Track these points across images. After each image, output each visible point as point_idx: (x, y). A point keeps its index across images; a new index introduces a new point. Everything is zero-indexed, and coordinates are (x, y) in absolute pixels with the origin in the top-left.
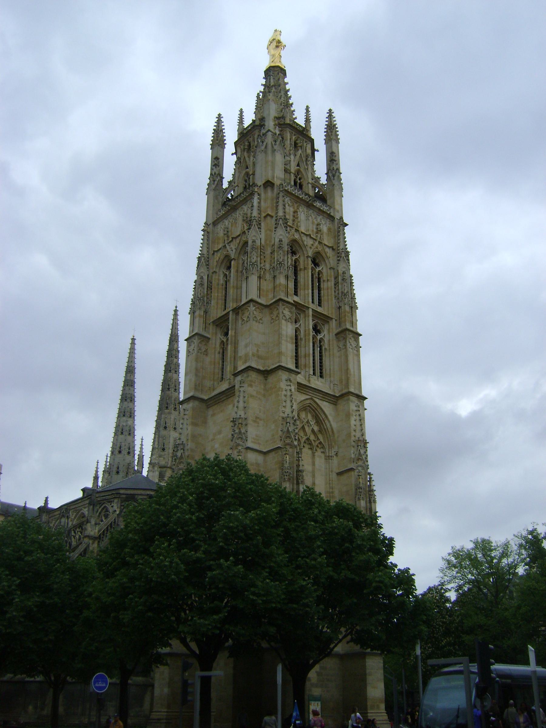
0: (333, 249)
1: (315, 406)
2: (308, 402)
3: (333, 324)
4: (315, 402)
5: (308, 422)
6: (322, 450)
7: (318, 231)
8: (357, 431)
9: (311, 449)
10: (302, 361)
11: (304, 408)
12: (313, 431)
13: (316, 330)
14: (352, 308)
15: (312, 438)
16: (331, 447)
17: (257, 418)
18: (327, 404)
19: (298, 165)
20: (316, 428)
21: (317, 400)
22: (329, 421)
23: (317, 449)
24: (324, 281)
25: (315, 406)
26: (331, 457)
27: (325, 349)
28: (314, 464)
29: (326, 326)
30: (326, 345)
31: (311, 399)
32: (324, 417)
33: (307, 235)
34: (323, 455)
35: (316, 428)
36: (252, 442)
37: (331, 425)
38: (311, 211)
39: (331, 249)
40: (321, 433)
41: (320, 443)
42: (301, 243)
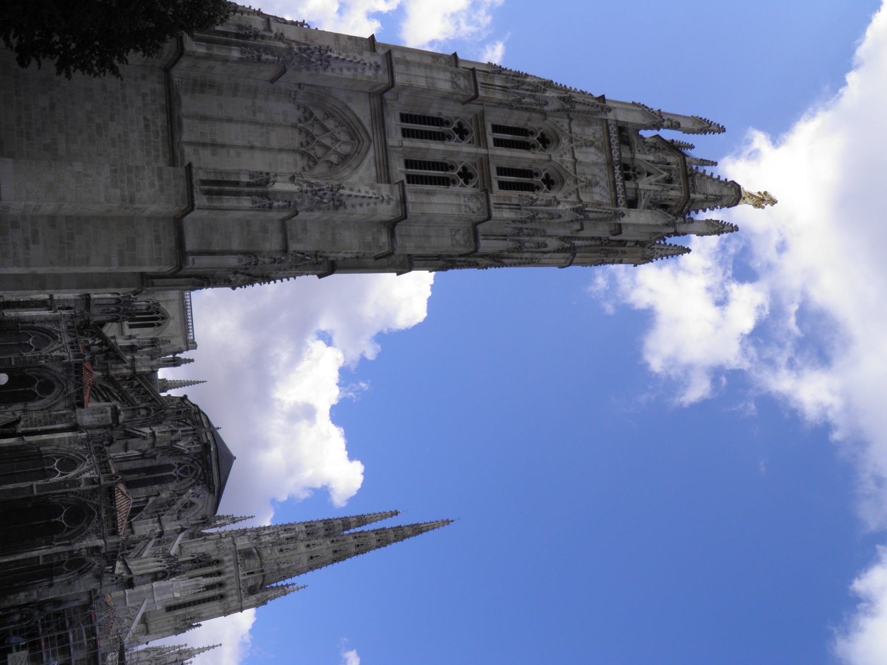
1: (363, 151)
2: (365, 139)
4: (369, 148)
5: (338, 140)
6: (307, 168)
7: (590, 184)
21: (371, 153)
25: (363, 151)
28: (280, 150)
30: (452, 188)
33: (574, 157)
34: (299, 170)
38: (606, 172)
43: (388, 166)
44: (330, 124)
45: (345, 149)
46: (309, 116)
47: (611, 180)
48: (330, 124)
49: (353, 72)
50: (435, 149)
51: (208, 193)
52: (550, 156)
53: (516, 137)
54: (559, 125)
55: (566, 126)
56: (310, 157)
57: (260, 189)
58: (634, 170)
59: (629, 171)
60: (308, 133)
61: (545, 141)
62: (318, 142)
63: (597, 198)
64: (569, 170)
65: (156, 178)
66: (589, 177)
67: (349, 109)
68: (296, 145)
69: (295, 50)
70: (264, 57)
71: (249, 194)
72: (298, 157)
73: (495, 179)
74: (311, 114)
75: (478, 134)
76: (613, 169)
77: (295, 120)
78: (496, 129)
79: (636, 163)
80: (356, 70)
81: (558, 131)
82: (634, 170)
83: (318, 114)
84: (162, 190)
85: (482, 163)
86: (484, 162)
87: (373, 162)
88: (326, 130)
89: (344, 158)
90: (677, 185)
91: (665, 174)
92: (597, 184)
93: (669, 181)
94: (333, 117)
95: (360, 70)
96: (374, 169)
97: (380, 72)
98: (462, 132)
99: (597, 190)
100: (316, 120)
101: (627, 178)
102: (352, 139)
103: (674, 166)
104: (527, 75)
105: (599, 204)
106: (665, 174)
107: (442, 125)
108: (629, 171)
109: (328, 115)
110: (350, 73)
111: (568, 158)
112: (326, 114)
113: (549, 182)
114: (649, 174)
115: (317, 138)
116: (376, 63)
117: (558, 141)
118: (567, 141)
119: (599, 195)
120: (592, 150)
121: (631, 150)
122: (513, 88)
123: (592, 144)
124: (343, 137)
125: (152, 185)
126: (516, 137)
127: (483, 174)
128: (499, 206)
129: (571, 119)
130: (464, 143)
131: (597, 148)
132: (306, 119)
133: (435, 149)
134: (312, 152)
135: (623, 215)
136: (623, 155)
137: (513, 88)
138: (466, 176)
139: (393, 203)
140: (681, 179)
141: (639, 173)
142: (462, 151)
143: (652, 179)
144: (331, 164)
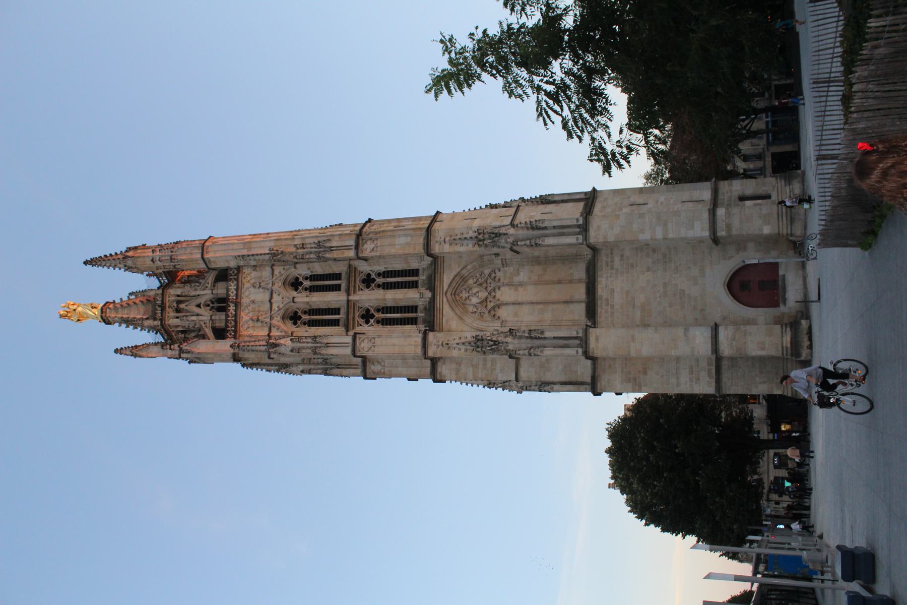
0: (273, 265)
6: (497, 271)
11: (459, 303)
13: (368, 281)
19: (199, 306)
23: (497, 279)
30: (382, 268)
41: (490, 275)
42: (282, 311)
53: (321, 317)
59: (220, 304)
71: (545, 228)
73: (343, 283)
78: (335, 323)
91: (182, 306)
93: (179, 302)
103: (172, 314)
104: (303, 372)
106: (182, 306)
107: (383, 319)
108: (220, 304)
122: (320, 347)
129: (269, 335)
130: (367, 305)
136: (223, 317)
140: (167, 305)
143: (198, 301)
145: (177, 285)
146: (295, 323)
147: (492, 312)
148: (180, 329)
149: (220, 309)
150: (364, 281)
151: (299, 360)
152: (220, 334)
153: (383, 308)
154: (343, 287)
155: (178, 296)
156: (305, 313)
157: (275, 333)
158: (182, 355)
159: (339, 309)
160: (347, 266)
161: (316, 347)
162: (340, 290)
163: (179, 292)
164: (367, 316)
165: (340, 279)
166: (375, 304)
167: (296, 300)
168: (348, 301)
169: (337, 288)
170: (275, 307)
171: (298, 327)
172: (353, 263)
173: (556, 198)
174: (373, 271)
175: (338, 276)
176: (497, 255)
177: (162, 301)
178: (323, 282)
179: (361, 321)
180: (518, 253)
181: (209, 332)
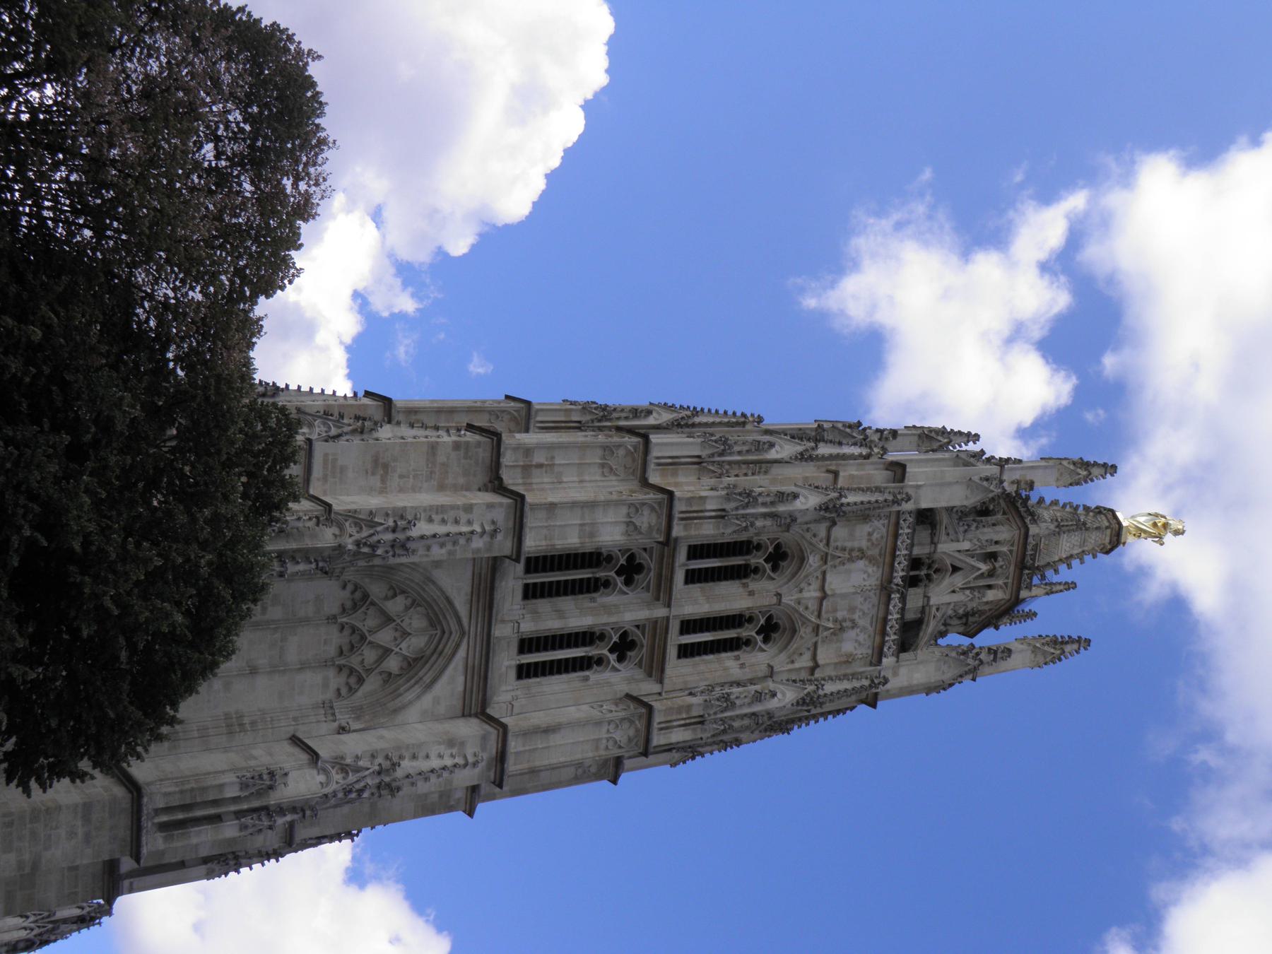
0: (812, 670)
1: (448, 651)
2: (454, 626)
3: (652, 687)
4: (458, 646)
6: (344, 691)
8: (415, 764)
9: (341, 653)
10: (544, 605)
12: (387, 652)
13: (624, 646)
14: (702, 723)
15: (370, 655)
16: (358, 712)
17: (386, 467)
18: (460, 688)
20: (393, 664)
21: (461, 653)
22: (418, 697)
24: (737, 658)
25: (448, 651)
26: (334, 714)
27: (586, 679)
28: (303, 666)
29: (639, 674)
30: (594, 675)
31: (463, 634)
32: (427, 679)
33: (822, 588)
34: (330, 694)
35: (393, 664)
36: (326, 455)
37: (411, 703)
38: (875, 600)
39: (810, 664)
40: (386, 682)
41: (361, 681)
42: (803, 574)
43: (486, 678)
44: (395, 606)
45: (415, 643)
46: (361, 600)
47: (881, 615)
48: (395, 606)
49: (449, 547)
50: (575, 615)
51: (163, 827)
52: (779, 595)
54: (808, 536)
55: (823, 534)
56: (352, 671)
57: (256, 804)
58: (929, 567)
60: (354, 630)
61: (778, 557)
62: (370, 643)
63: (848, 647)
64: (806, 614)
65: (79, 823)
66: (840, 615)
67: (434, 583)
68: (332, 651)
69: (350, 547)
70: (292, 568)
72: (331, 673)
73: (676, 639)
74: (366, 596)
75: (659, 576)
76: (889, 599)
77: (335, 610)
78: (696, 551)
79: (936, 557)
80: (455, 543)
81: (805, 545)
82: (929, 567)
83: (377, 590)
84: (87, 838)
85: (655, 629)
86: (658, 629)
87: (461, 668)
88: (388, 619)
89: (413, 664)
90: (1000, 582)
92: (854, 625)
93: (991, 574)
94: (403, 592)
95: (462, 541)
96: (461, 679)
97: (500, 537)
98: (631, 569)
99: (852, 634)
100: (373, 603)
101: (913, 582)
102: (432, 625)
103: (1005, 549)
105: (849, 660)
106: (984, 567)
109: (395, 592)
110: (443, 551)
111: (812, 593)
112: (391, 588)
113: (769, 629)
114: (955, 569)
115: (369, 638)
116: (493, 522)
117: (803, 560)
118: (818, 557)
119: (856, 643)
120: (861, 564)
121: (933, 535)
122: (737, 509)
123: (862, 554)
124: (416, 621)
125: (72, 834)
126: (726, 559)
127: (661, 568)
128: (666, 727)
130: (632, 596)
131: (871, 560)
132: (355, 607)
133: (575, 615)
134: (354, 661)
135: (886, 681)
137: (737, 509)
138: (624, 646)
139: (482, 765)
140: (1012, 568)
141: (937, 571)
142: (624, 609)
143: (958, 580)
144: (388, 677)
145: (986, 608)
146: (778, 547)
147: (358, 595)
148: (990, 519)
149: (915, 563)
150: (632, 645)
151: (776, 471)
152: (926, 518)
153: (596, 590)
154: (675, 627)
155: (990, 587)
156: (756, 570)
157: (822, 530)
158: (995, 470)
159: (687, 582)
160: (666, 681)
161: (747, 506)
162: (682, 622)
163: (991, 595)
164: (631, 569)
165: (680, 646)
166: (611, 599)
167: (774, 600)
168: (669, 606)
169: (688, 626)
170: (815, 585)
171: (772, 541)
172: (656, 688)
173: (203, 869)
174: (615, 669)
175: (686, 651)
176: (342, 730)
177: (1021, 575)
178: (719, 635)
179: (643, 558)
180: (296, 741)
181: (945, 519)
